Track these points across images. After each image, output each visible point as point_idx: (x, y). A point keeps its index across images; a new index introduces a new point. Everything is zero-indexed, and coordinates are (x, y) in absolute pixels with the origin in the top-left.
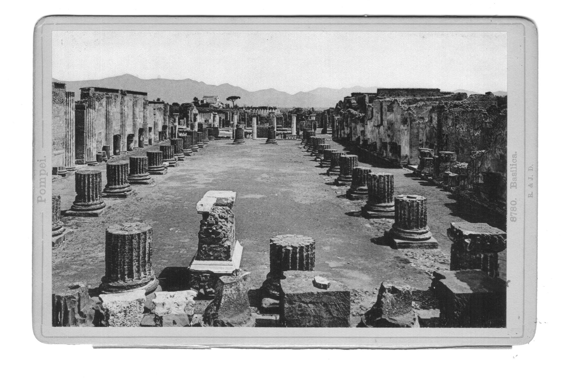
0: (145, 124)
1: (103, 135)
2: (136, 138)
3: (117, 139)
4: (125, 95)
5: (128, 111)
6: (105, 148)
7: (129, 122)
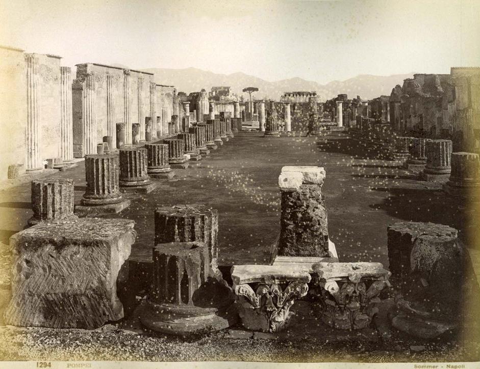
0: (152, 112)
1: (104, 123)
2: (142, 129)
3: (119, 127)
4: (128, 74)
5: (132, 95)
6: (105, 139)
7: (134, 108)
